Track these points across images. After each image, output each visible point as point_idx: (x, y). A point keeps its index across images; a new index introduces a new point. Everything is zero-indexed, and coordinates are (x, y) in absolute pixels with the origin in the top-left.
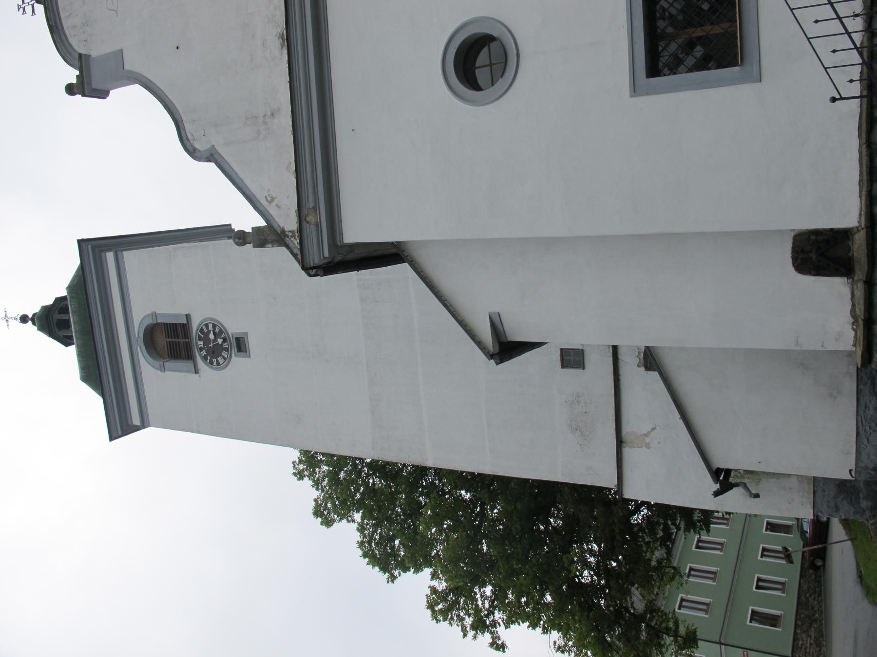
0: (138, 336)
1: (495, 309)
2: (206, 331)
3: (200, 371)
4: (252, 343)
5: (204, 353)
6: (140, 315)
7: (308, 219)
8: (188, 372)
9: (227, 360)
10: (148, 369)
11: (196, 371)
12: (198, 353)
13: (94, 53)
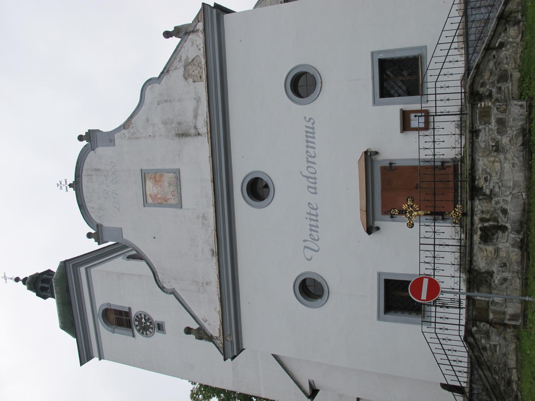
0: (99, 312)
1: (312, 378)
2: (140, 317)
3: (136, 336)
4: (167, 327)
5: (138, 328)
6: (100, 302)
7: (227, 339)
8: (129, 335)
9: (152, 334)
10: (105, 331)
11: (134, 336)
12: (135, 328)
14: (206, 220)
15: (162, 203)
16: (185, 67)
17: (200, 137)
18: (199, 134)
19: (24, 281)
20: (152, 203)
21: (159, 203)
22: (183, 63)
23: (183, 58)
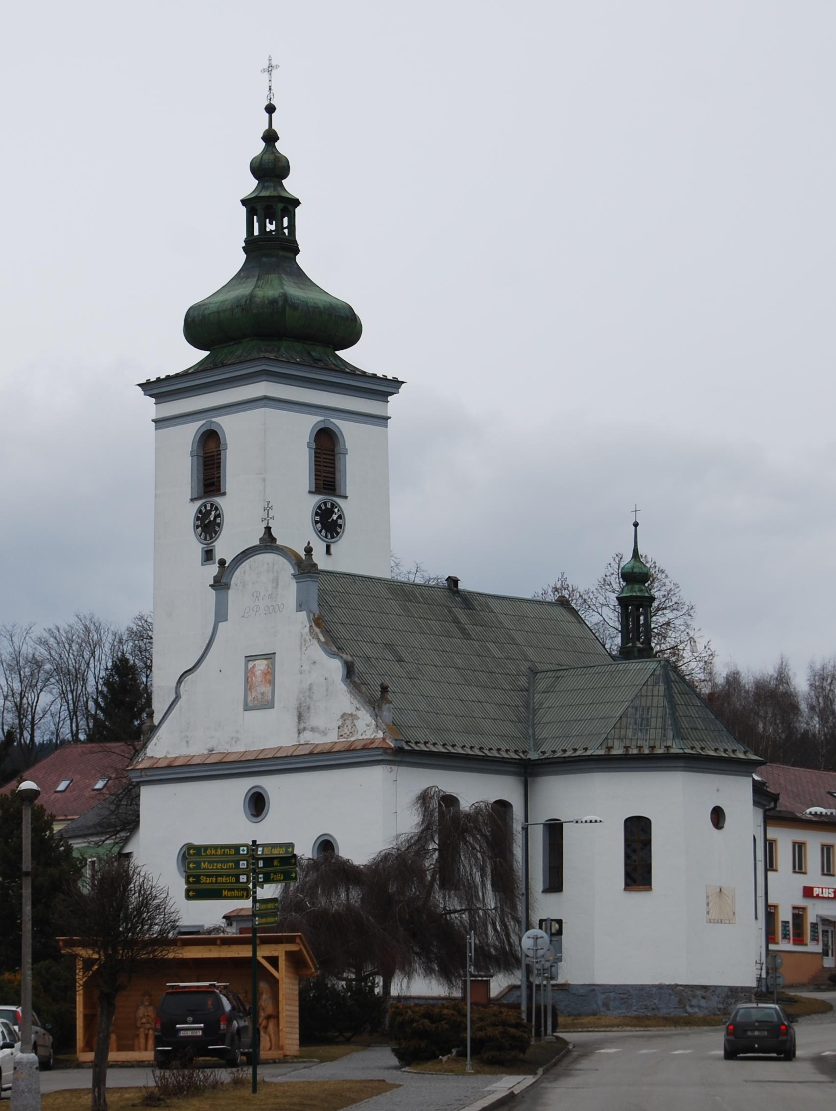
3: (192, 503)
11: (192, 500)
13: (230, 591)
14: (235, 742)
15: (249, 685)
16: (351, 715)
17: (297, 735)
18: (299, 733)
19: (270, 137)
20: (248, 668)
21: (248, 678)
22: (354, 713)
23: (359, 714)
